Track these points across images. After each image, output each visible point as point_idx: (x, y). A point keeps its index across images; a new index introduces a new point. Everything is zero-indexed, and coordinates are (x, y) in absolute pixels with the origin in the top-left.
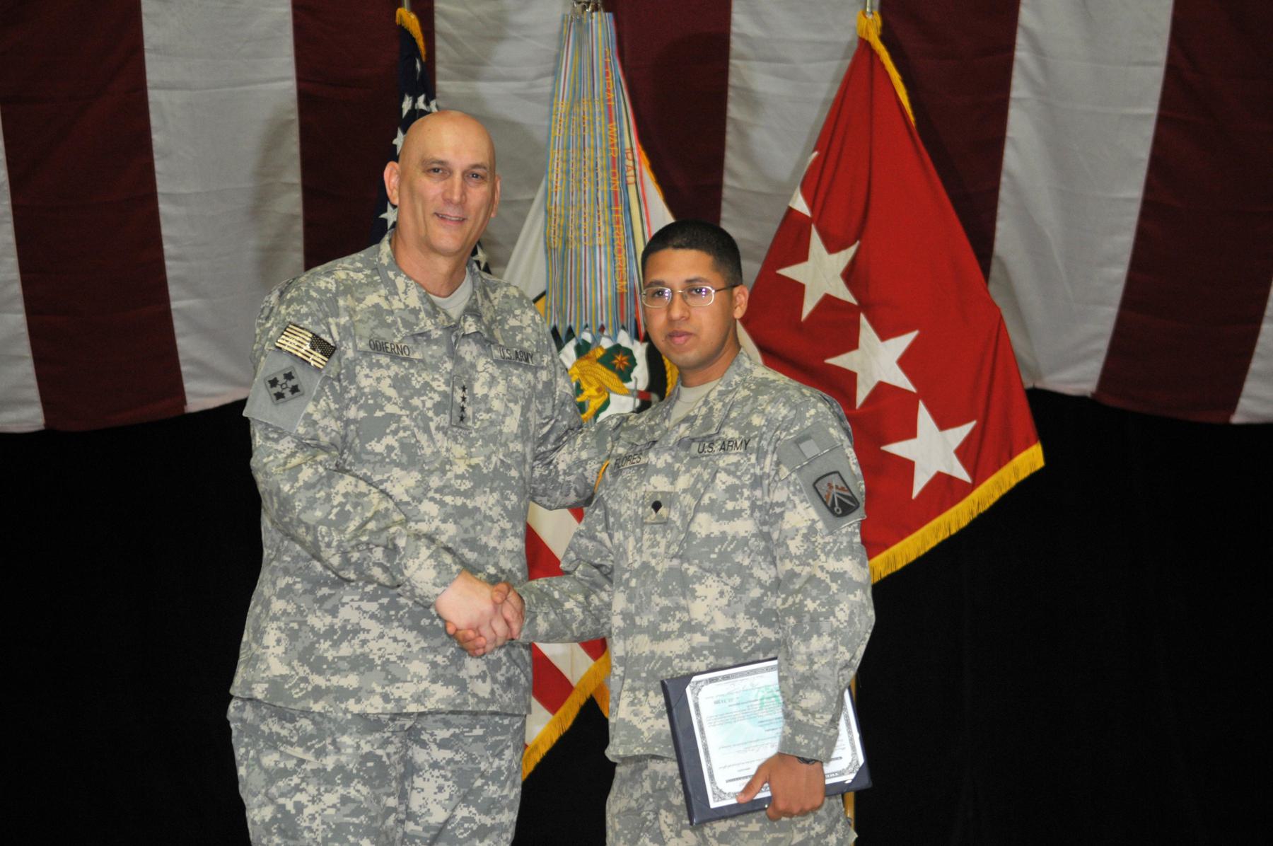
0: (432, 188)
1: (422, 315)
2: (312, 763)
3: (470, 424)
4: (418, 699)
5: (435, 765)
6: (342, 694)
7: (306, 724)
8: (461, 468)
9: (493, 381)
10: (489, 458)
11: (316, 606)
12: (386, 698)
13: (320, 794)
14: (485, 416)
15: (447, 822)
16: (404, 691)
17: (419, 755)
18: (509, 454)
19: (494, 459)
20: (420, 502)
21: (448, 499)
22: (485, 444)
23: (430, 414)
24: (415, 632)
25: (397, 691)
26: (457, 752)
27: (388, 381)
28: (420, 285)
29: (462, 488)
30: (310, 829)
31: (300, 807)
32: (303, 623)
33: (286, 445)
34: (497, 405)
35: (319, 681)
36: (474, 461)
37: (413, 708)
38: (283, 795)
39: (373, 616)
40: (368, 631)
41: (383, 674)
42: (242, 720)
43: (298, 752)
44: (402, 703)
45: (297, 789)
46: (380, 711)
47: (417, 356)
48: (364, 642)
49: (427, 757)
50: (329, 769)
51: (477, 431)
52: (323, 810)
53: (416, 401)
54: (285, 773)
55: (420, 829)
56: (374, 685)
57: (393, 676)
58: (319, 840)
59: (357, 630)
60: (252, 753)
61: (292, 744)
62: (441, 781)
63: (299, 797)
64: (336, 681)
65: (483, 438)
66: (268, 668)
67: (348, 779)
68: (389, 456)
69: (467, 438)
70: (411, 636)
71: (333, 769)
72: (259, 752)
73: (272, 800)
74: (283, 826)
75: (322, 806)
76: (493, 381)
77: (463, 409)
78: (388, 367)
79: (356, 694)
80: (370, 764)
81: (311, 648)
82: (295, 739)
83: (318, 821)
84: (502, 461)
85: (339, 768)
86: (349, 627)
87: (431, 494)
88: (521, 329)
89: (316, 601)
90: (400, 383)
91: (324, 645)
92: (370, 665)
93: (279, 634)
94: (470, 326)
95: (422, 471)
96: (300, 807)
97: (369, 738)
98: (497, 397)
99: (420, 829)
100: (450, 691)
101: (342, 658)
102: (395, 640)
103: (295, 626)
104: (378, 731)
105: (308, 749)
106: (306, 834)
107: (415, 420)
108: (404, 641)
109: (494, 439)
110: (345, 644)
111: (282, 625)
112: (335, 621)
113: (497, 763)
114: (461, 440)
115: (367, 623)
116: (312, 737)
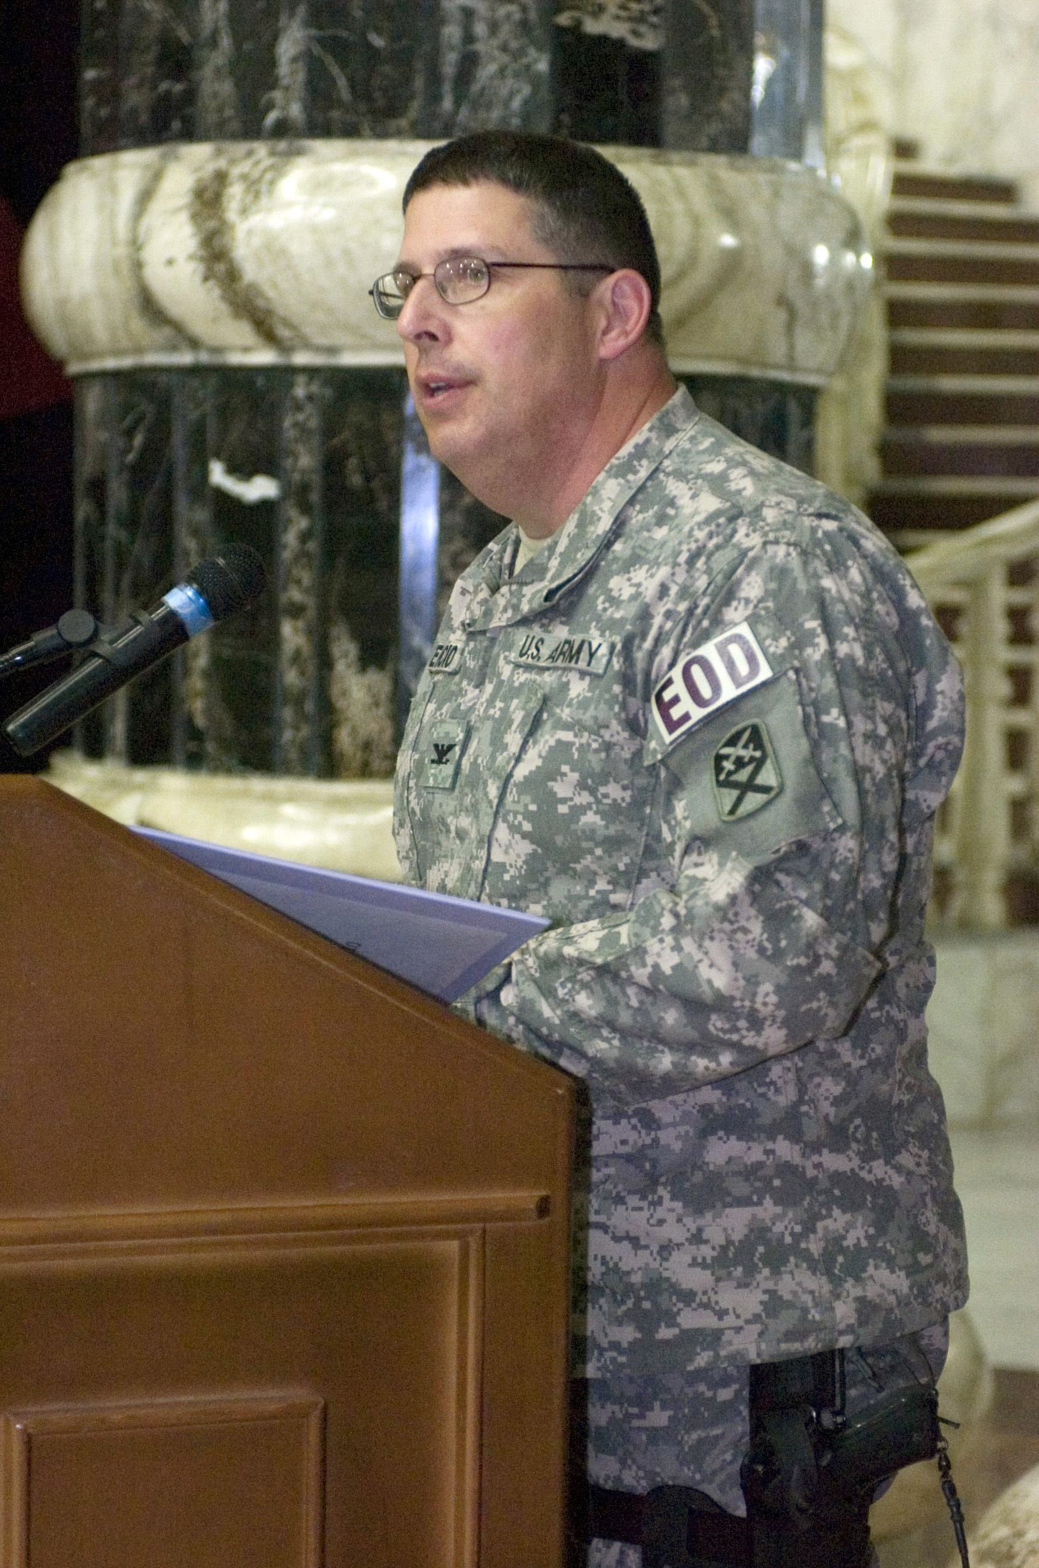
39: (688, 1297)
48: (697, 1238)
86: (739, 1271)
108: (617, 1239)
112: (770, 1285)
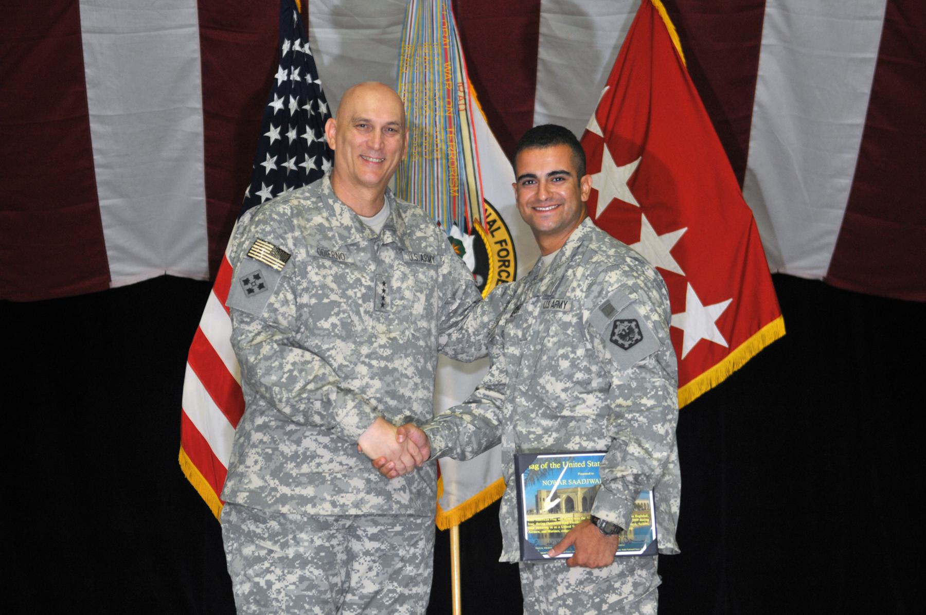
0: (358, 137)
1: (353, 231)
2: (278, 553)
3: (388, 308)
4: (357, 505)
5: (367, 553)
6: (303, 500)
7: (274, 525)
8: (383, 340)
9: (404, 277)
10: (403, 332)
11: (286, 438)
12: (334, 504)
13: (284, 575)
14: (399, 302)
15: (377, 593)
16: (347, 499)
17: (356, 546)
18: (418, 330)
19: (407, 333)
20: (356, 364)
21: (374, 363)
22: (400, 323)
23: (360, 302)
24: (355, 459)
25: (343, 499)
26: (383, 543)
27: (331, 278)
28: (351, 209)
29: (385, 354)
31: (269, 584)
32: (275, 449)
33: (255, 327)
34: (408, 294)
35: (286, 490)
36: (392, 335)
37: (353, 511)
38: (257, 575)
39: (325, 447)
40: (322, 457)
41: (332, 487)
42: (229, 522)
43: (268, 544)
44: (345, 508)
45: (268, 571)
46: (329, 513)
47: (350, 260)
48: (319, 465)
49: (361, 547)
50: (291, 556)
51: (394, 313)
52: (287, 586)
53: (350, 293)
54: (259, 560)
55: (357, 598)
56: (325, 495)
57: (339, 489)
58: (284, 607)
59: (314, 456)
60: (235, 545)
61: (264, 539)
62: (371, 563)
63: (269, 577)
64: (298, 491)
65: (398, 318)
66: (250, 482)
67: (304, 564)
68: (333, 331)
69: (387, 318)
71: (294, 557)
72: (241, 545)
73: (249, 579)
74: (258, 598)
75: (285, 583)
76: (404, 277)
77: (383, 298)
78: (331, 268)
79: (312, 501)
80: (323, 554)
81: (280, 468)
82: (266, 535)
83: (283, 594)
84: (413, 335)
85: (298, 556)
86: (308, 453)
87: (363, 359)
88: (425, 238)
89: (286, 434)
90: (339, 279)
91: (290, 466)
92: (324, 481)
93: (257, 457)
94: (388, 238)
95: (355, 342)
96: (269, 584)
97: (320, 535)
98: (408, 288)
99: (357, 598)
100: (380, 500)
101: (303, 475)
102: (341, 464)
103: (270, 451)
104: (326, 529)
105: (276, 542)
106: (274, 603)
107: (350, 306)
109: (407, 319)
111: (259, 450)
112: (299, 448)
113: (412, 550)
114: (382, 320)
115: (321, 451)
116: (278, 534)
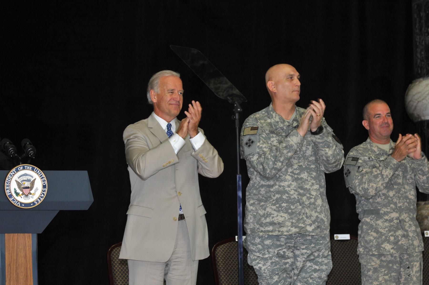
11: (261, 208)
30: (265, 273)
39: (275, 210)
48: (273, 217)
59: (271, 214)
70: (286, 215)
81: (260, 220)
83: (266, 270)
89: (261, 206)
101: (267, 222)
102: (281, 216)
103: (255, 214)
106: (264, 274)
110: (268, 218)
115: (273, 212)
